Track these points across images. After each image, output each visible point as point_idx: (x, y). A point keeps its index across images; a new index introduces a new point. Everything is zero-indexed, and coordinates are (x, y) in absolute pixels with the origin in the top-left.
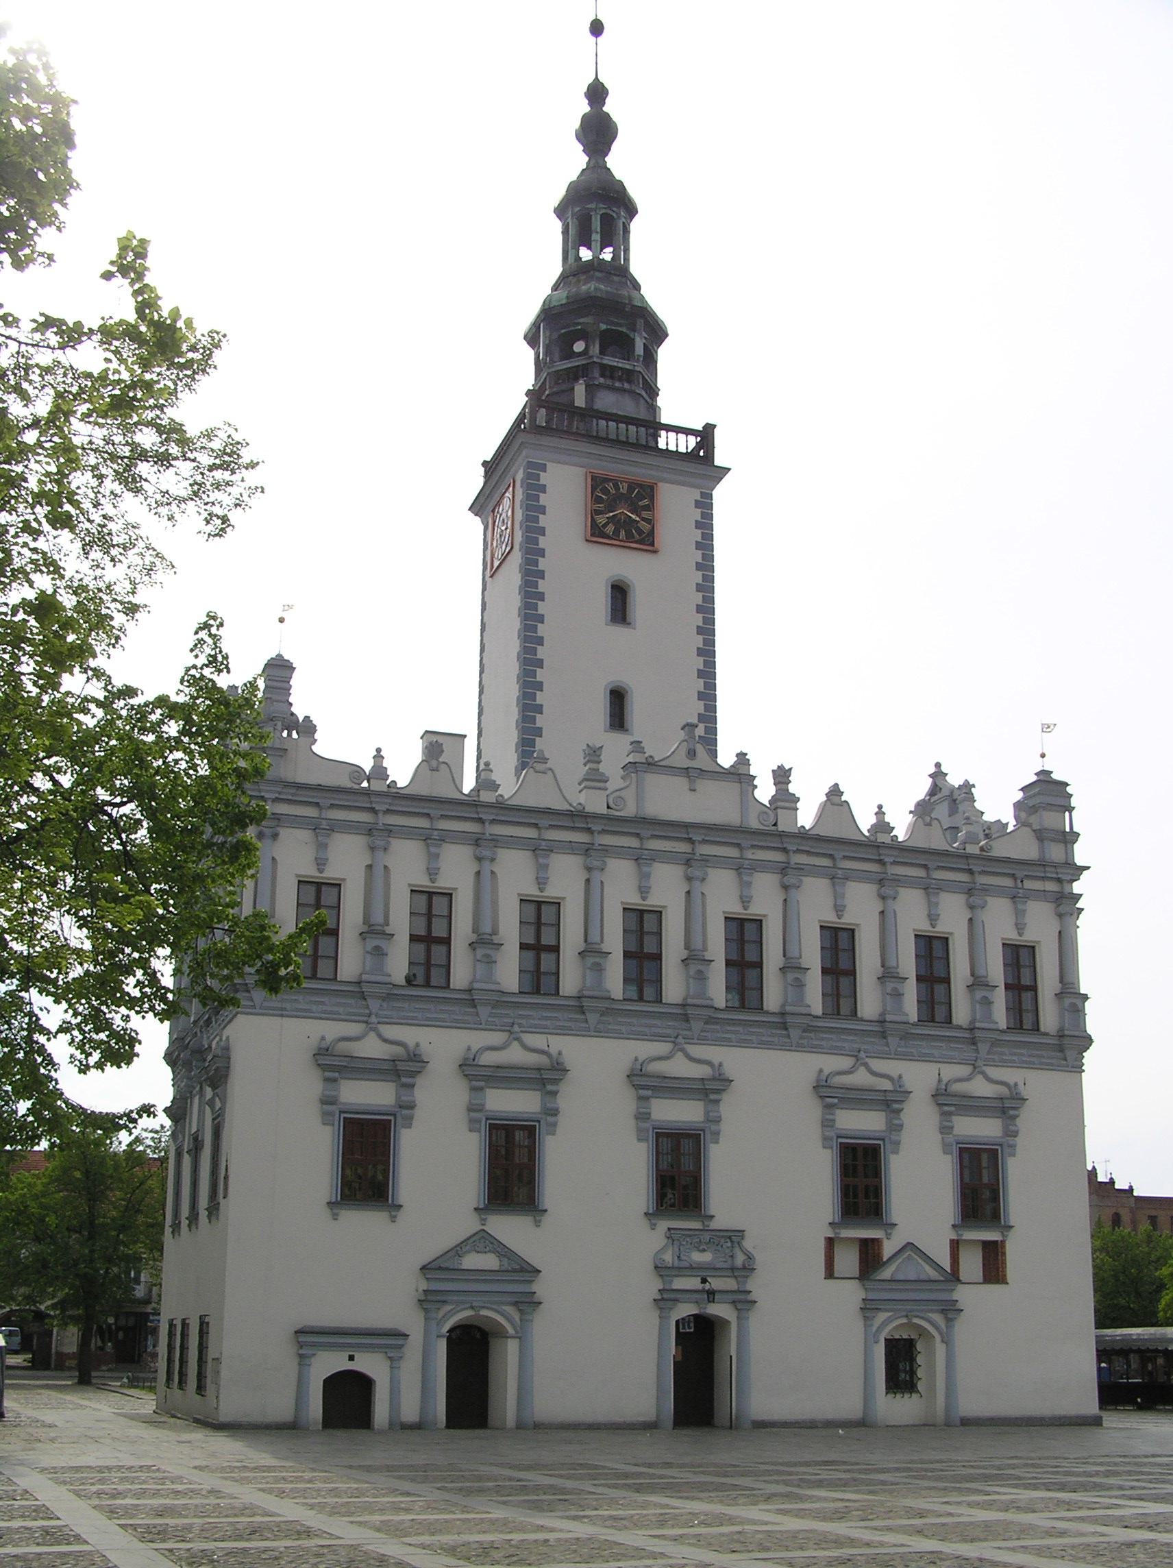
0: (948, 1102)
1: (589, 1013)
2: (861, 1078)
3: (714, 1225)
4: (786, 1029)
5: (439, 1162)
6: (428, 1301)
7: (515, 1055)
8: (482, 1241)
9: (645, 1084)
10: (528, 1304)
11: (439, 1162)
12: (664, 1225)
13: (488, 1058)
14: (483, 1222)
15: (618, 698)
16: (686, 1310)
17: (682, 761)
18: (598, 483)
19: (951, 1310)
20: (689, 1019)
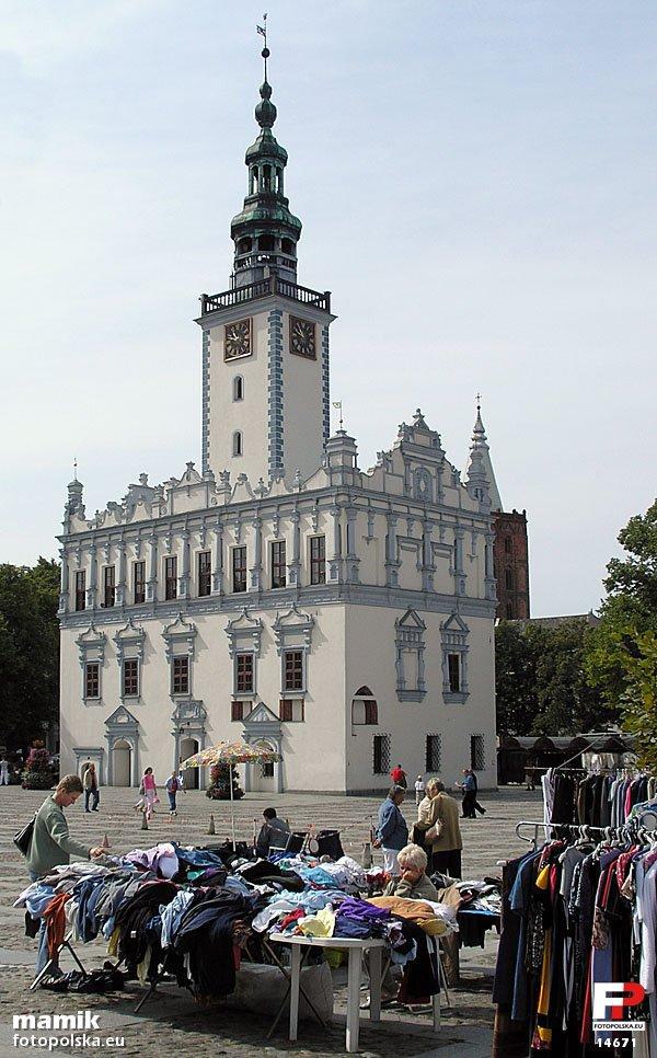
0: (283, 631)
1: (157, 611)
2: (246, 623)
3: (196, 697)
4: (224, 604)
5: (111, 678)
6: (110, 736)
7: (131, 633)
8: (121, 711)
9: (171, 639)
10: (137, 735)
11: (111, 678)
12: (176, 699)
13: (123, 635)
14: (123, 702)
15: (238, 437)
16: (184, 737)
17: (185, 483)
18: (228, 330)
19: (280, 736)
20: (190, 606)
